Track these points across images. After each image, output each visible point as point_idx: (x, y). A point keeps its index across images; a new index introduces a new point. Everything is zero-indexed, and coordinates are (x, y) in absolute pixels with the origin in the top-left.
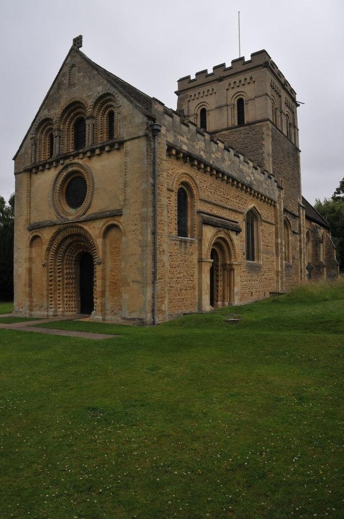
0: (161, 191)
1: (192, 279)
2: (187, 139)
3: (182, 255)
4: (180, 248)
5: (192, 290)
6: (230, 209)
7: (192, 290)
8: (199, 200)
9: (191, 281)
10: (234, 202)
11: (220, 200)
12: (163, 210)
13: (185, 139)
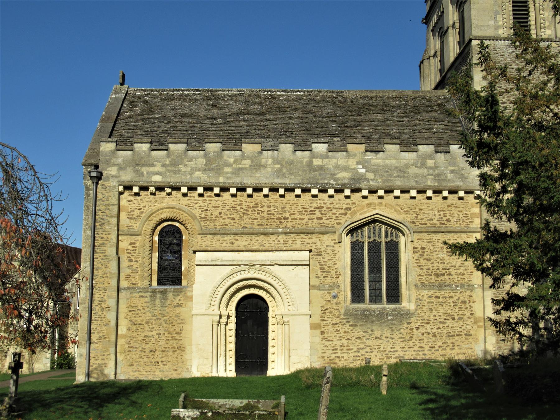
0: (106, 240)
1: (178, 338)
2: (163, 165)
3: (156, 308)
4: (152, 300)
5: (178, 352)
6: (286, 233)
7: (178, 352)
8: (199, 234)
9: (176, 339)
10: (303, 219)
11: (258, 225)
12: (108, 262)
13: (158, 169)
